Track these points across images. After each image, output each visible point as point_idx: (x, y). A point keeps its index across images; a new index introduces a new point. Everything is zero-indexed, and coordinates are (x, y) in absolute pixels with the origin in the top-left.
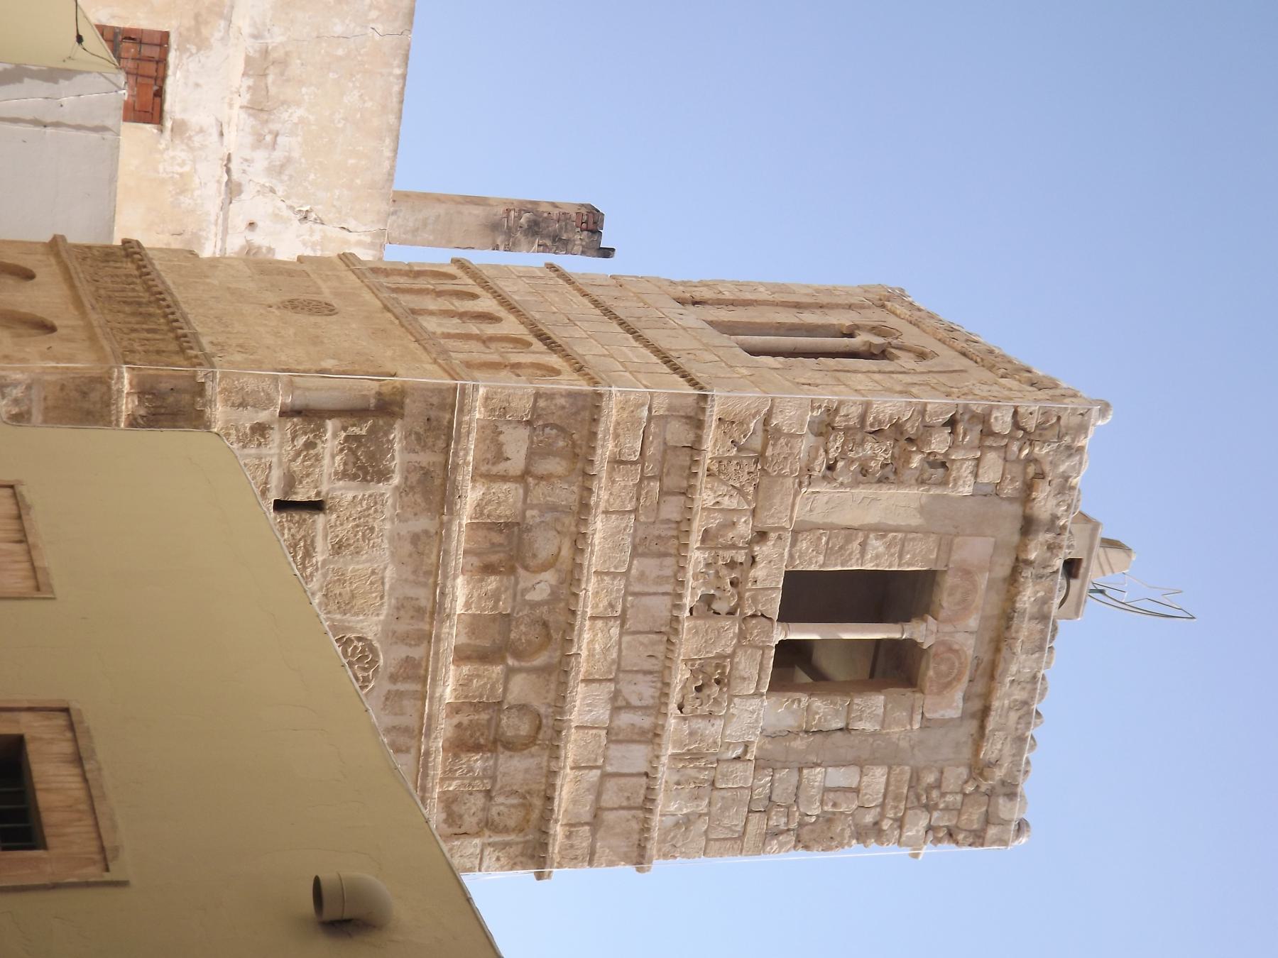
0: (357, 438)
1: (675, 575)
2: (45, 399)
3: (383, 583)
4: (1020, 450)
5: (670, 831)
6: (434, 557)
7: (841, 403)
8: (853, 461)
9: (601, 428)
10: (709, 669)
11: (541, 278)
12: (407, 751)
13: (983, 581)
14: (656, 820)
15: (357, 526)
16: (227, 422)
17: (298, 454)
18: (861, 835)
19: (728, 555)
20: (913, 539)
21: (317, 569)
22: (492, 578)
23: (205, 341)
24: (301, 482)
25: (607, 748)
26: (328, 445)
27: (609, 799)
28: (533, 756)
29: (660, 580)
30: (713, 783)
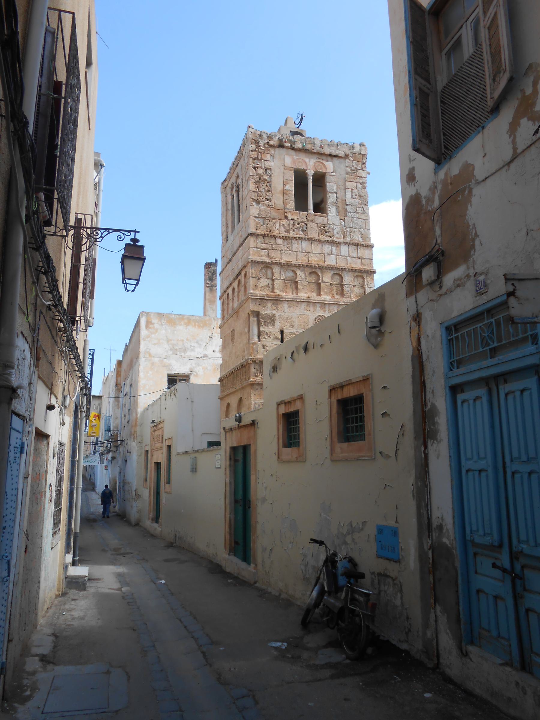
0: (265, 322)
18: (365, 188)
19: (291, 226)
23: (242, 361)
27: (355, 255)
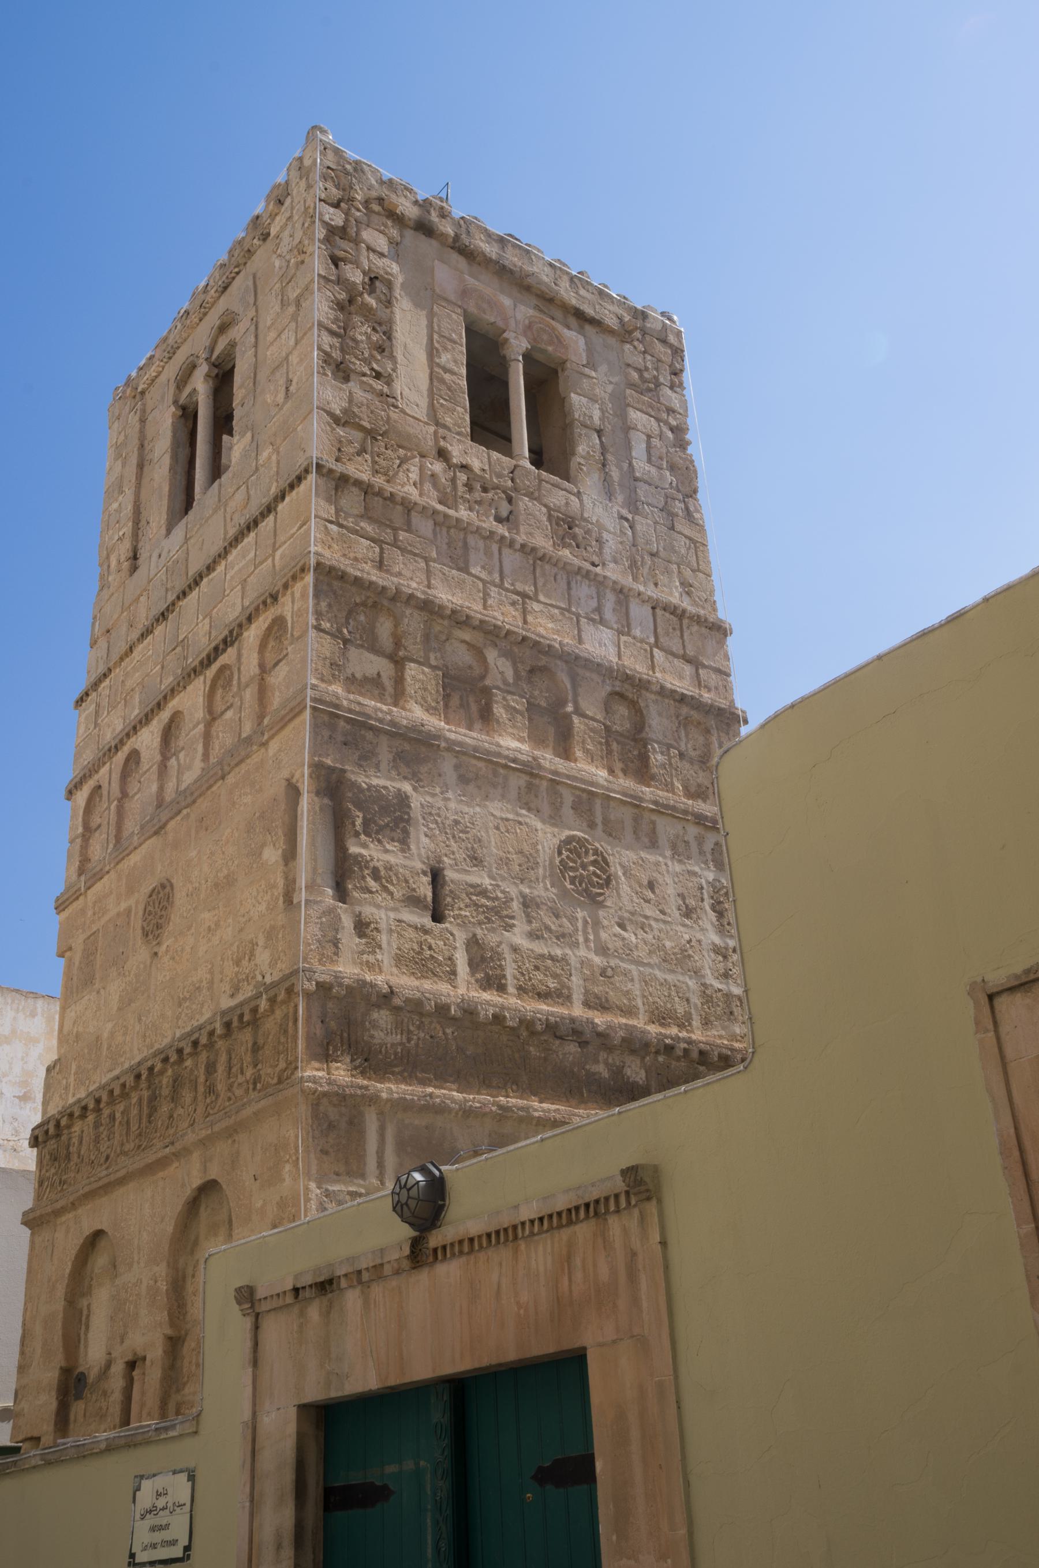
0: (366, 823)
1: (485, 538)
2: (337, 1174)
3: (507, 820)
4: (358, 210)
5: (695, 601)
6: (481, 764)
7: (319, 349)
8: (372, 356)
9: (350, 570)
10: (561, 533)
11: (98, 705)
12: (654, 823)
13: (471, 281)
14: (691, 609)
15: (454, 837)
16: (354, 963)
17: (385, 889)
18: (682, 444)
19: (461, 489)
20: (439, 326)
21: (498, 886)
22: (495, 710)
23: (226, 1003)
24: (414, 890)
25: (634, 638)
26: (375, 854)
27: (676, 646)
28: (647, 706)
29: (488, 553)
30: (652, 555)
